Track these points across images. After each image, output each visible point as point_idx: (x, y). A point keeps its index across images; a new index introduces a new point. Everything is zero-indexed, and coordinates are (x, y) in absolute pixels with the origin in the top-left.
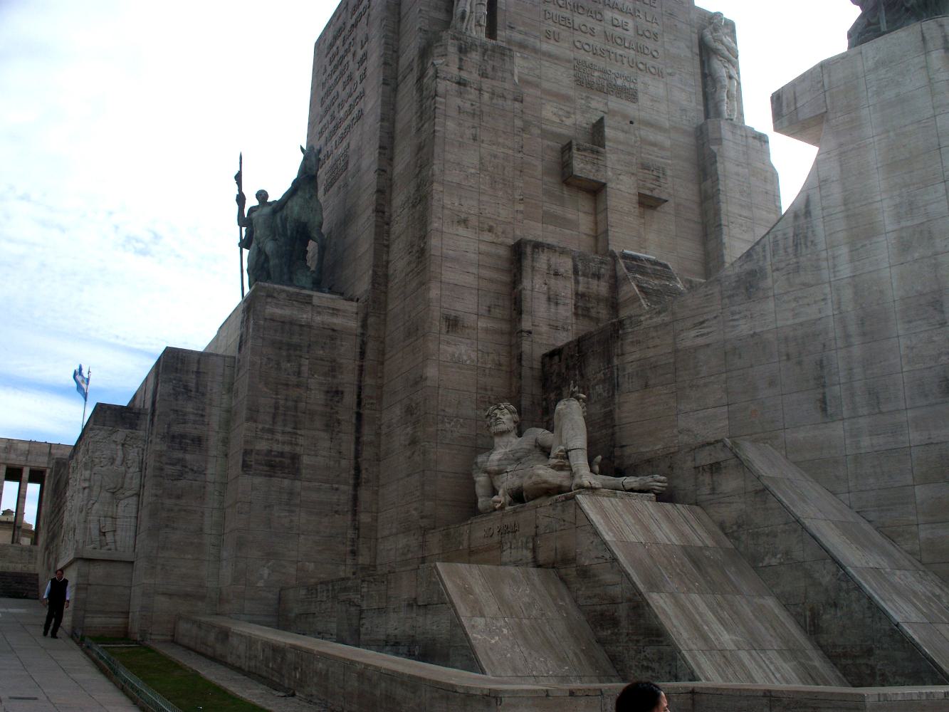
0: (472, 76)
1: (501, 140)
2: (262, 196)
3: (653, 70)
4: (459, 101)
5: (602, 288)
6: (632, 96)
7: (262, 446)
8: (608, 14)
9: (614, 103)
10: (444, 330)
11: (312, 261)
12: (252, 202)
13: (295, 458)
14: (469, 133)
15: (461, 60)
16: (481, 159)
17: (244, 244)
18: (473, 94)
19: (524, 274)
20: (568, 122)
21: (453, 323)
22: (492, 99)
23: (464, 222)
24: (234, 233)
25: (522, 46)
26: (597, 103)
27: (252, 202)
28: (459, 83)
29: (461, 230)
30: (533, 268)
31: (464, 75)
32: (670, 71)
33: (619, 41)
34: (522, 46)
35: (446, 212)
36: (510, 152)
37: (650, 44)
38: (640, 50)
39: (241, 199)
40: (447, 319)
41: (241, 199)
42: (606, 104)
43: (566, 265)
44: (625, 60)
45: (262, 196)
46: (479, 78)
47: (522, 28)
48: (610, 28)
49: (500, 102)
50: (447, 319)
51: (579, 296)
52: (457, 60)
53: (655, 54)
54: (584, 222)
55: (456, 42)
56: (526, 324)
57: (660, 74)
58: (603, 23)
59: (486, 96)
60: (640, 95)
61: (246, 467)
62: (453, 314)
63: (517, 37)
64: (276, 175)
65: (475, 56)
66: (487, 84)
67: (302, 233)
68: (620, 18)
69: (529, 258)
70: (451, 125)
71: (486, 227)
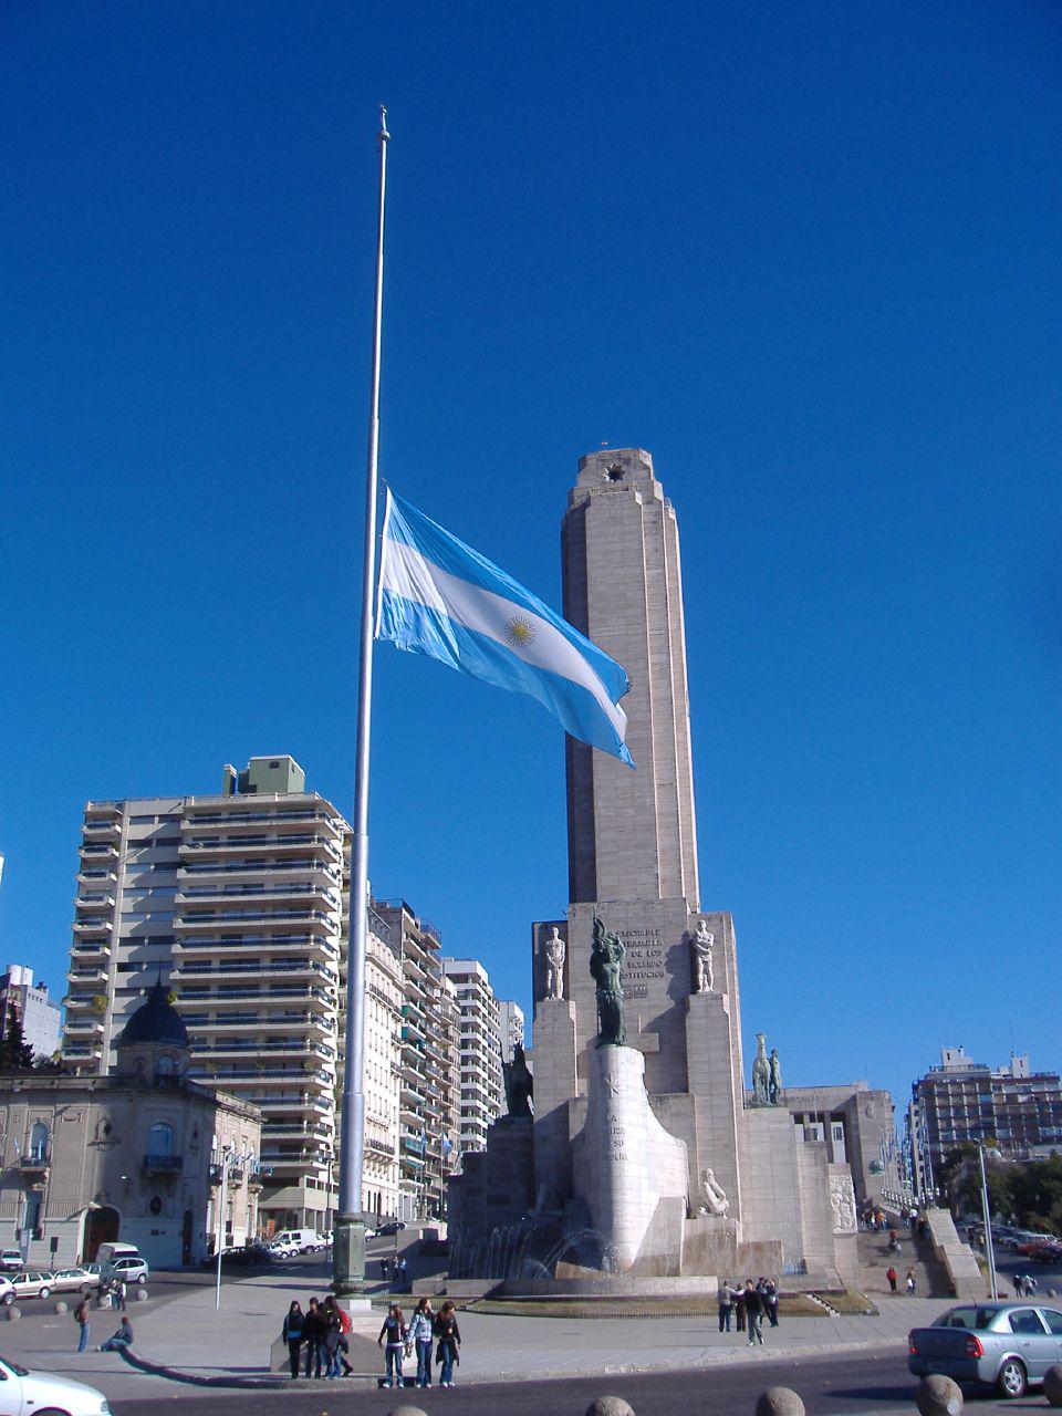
21: (545, 1139)
38: (649, 965)
61: (489, 1203)
63: (578, 985)
65: (549, 1011)
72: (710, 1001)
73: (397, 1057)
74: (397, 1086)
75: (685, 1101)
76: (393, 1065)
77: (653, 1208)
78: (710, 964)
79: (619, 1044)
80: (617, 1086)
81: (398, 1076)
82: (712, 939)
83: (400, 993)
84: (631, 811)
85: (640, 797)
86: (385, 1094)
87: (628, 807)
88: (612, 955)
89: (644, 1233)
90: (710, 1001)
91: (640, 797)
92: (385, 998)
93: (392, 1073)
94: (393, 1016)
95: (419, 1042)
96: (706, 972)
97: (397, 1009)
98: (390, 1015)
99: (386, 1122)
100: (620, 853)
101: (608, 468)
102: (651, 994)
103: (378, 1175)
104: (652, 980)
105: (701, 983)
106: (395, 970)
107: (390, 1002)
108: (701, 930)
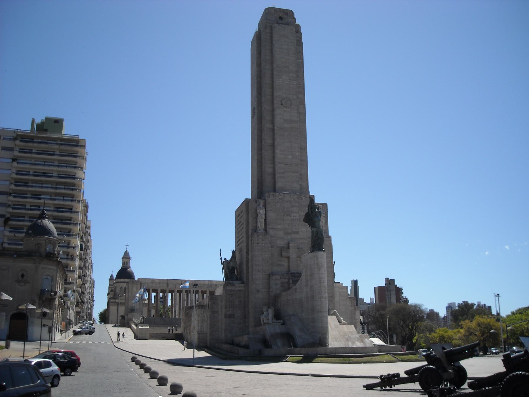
2: (225, 259)
5: (286, 280)
6: (297, 233)
7: (228, 313)
8: (292, 214)
9: (294, 236)
11: (236, 273)
12: (223, 260)
13: (234, 315)
17: (223, 269)
20: (282, 243)
24: (221, 266)
25: (272, 228)
26: (289, 237)
27: (223, 260)
34: (272, 228)
39: (221, 259)
41: (221, 259)
43: (278, 277)
45: (225, 259)
51: (281, 283)
54: (286, 264)
56: (271, 290)
63: (271, 227)
64: (228, 256)
65: (261, 237)
67: (233, 268)
70: (256, 253)
84: (290, 157)
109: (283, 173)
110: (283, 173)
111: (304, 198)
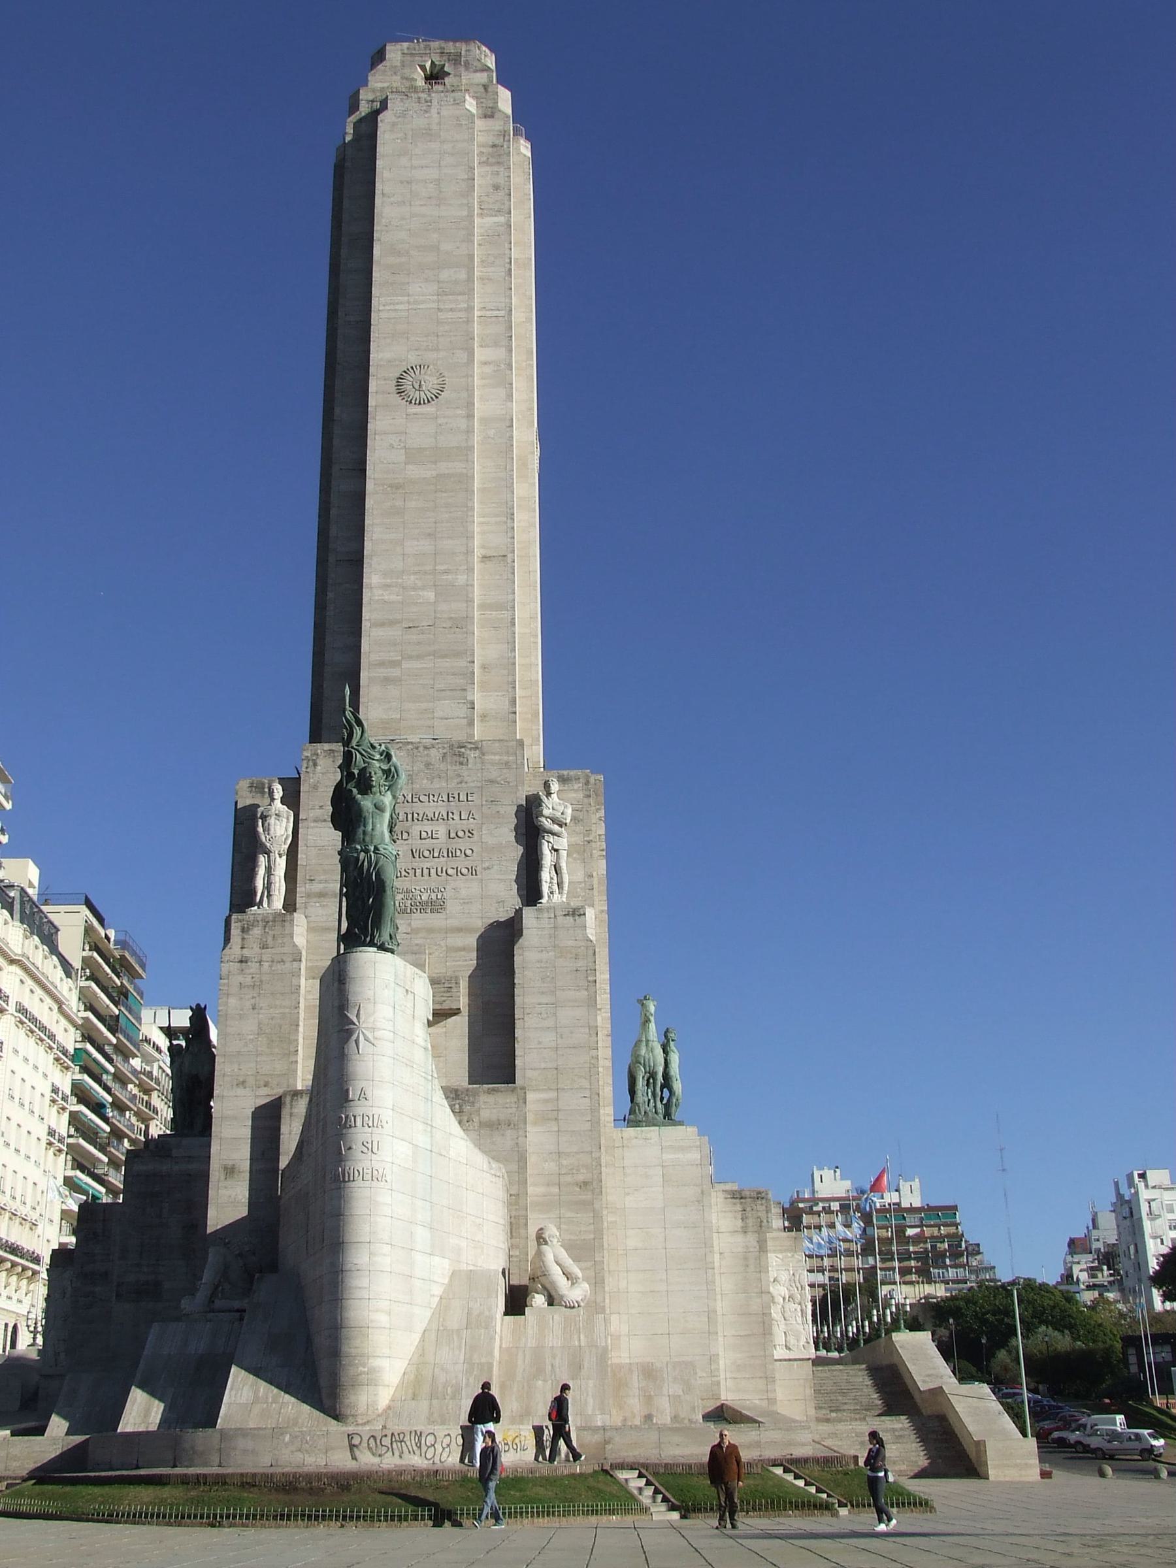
0: (252, 951)
1: (278, 1003)
3: (464, 871)
4: (240, 978)
6: (436, 906)
10: (223, 1177)
14: (248, 1004)
15: (243, 939)
16: (259, 1024)
18: (253, 967)
19: (283, 1121)
22: (271, 966)
23: (243, 1083)
28: (241, 961)
29: (240, 1091)
30: (291, 1115)
31: (246, 952)
32: (486, 865)
33: (426, 853)
35: (226, 1079)
36: (287, 1010)
37: (464, 844)
38: (451, 854)
40: (226, 1168)
42: (410, 924)
44: (433, 871)
46: (260, 951)
47: (322, 877)
48: (416, 843)
49: (279, 966)
50: (226, 1168)
52: (240, 941)
53: (469, 852)
55: (239, 924)
57: (473, 871)
58: (409, 842)
59: (266, 965)
60: (448, 903)
62: (231, 1163)
65: (257, 931)
66: (267, 955)
68: (428, 827)
69: (288, 1106)
71: (262, 1083)
72: (560, 919)
73: (62, 1125)
74: (61, 1167)
75: (511, 1099)
76: (52, 1133)
77: (438, 1290)
78: (564, 854)
79: (382, 948)
80: (373, 1029)
81: (60, 1151)
82: (569, 811)
83: (72, 1030)
84: (430, 595)
85: (446, 572)
86: (35, 1174)
87: (423, 588)
88: (377, 778)
89: (417, 1337)
90: (560, 919)
91: (446, 572)
92: (43, 1029)
93: (50, 1144)
94: (57, 1059)
95: (102, 1106)
96: (557, 869)
97: (65, 1053)
98: (52, 1057)
99: (33, 1216)
100: (405, 665)
101: (423, 68)
102: (452, 907)
103: (15, 1297)
104: (460, 882)
105: (545, 888)
106: (65, 992)
107: (52, 1037)
108: (549, 794)
109: (395, 664)
110: (395, 664)
111: (472, 754)
